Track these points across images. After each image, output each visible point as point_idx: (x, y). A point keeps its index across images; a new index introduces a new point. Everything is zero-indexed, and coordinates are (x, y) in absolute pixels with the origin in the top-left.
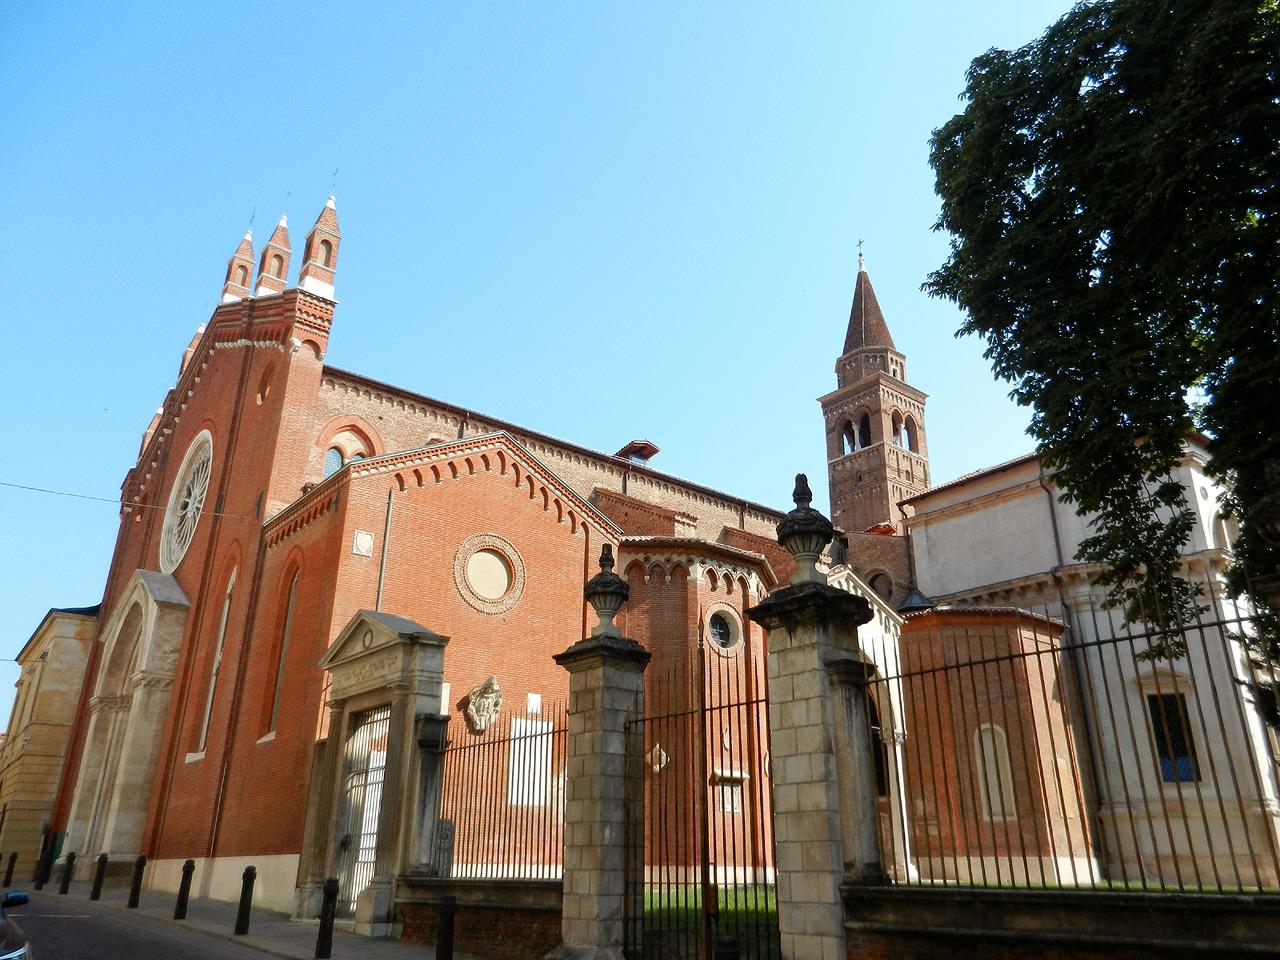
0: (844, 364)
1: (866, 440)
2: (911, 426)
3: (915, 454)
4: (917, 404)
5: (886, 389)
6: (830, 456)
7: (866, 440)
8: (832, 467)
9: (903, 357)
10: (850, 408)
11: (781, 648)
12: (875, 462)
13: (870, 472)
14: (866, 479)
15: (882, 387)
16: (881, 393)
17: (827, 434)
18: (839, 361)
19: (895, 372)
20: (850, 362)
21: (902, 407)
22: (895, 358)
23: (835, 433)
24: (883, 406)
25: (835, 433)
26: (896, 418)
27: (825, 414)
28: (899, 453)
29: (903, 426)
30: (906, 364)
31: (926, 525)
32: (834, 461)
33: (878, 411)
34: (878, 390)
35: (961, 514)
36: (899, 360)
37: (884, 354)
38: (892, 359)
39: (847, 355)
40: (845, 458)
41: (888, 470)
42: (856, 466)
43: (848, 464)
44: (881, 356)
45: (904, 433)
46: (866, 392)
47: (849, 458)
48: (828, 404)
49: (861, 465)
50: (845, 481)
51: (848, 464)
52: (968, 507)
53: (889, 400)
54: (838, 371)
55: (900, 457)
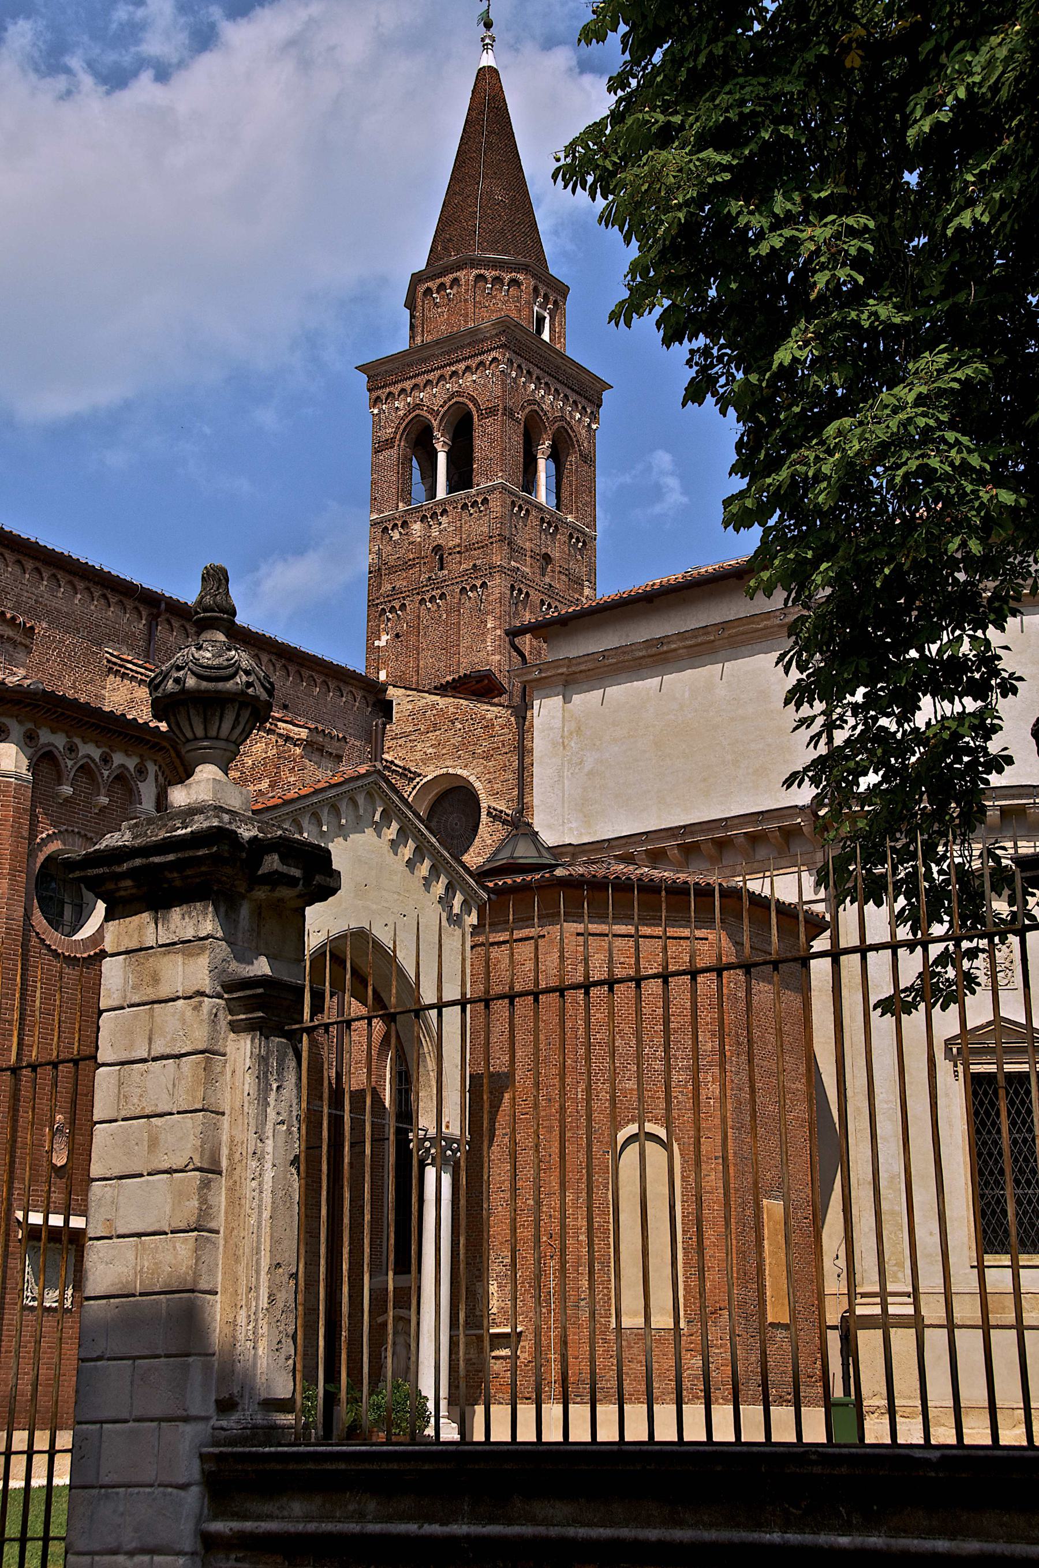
0: (429, 291)
9: (563, 291)
10: (434, 398)
11: (134, 945)
17: (377, 451)
20: (442, 287)
23: (391, 455)
25: (391, 455)
30: (570, 304)
46: (473, 363)
49: (444, 531)
50: (407, 565)
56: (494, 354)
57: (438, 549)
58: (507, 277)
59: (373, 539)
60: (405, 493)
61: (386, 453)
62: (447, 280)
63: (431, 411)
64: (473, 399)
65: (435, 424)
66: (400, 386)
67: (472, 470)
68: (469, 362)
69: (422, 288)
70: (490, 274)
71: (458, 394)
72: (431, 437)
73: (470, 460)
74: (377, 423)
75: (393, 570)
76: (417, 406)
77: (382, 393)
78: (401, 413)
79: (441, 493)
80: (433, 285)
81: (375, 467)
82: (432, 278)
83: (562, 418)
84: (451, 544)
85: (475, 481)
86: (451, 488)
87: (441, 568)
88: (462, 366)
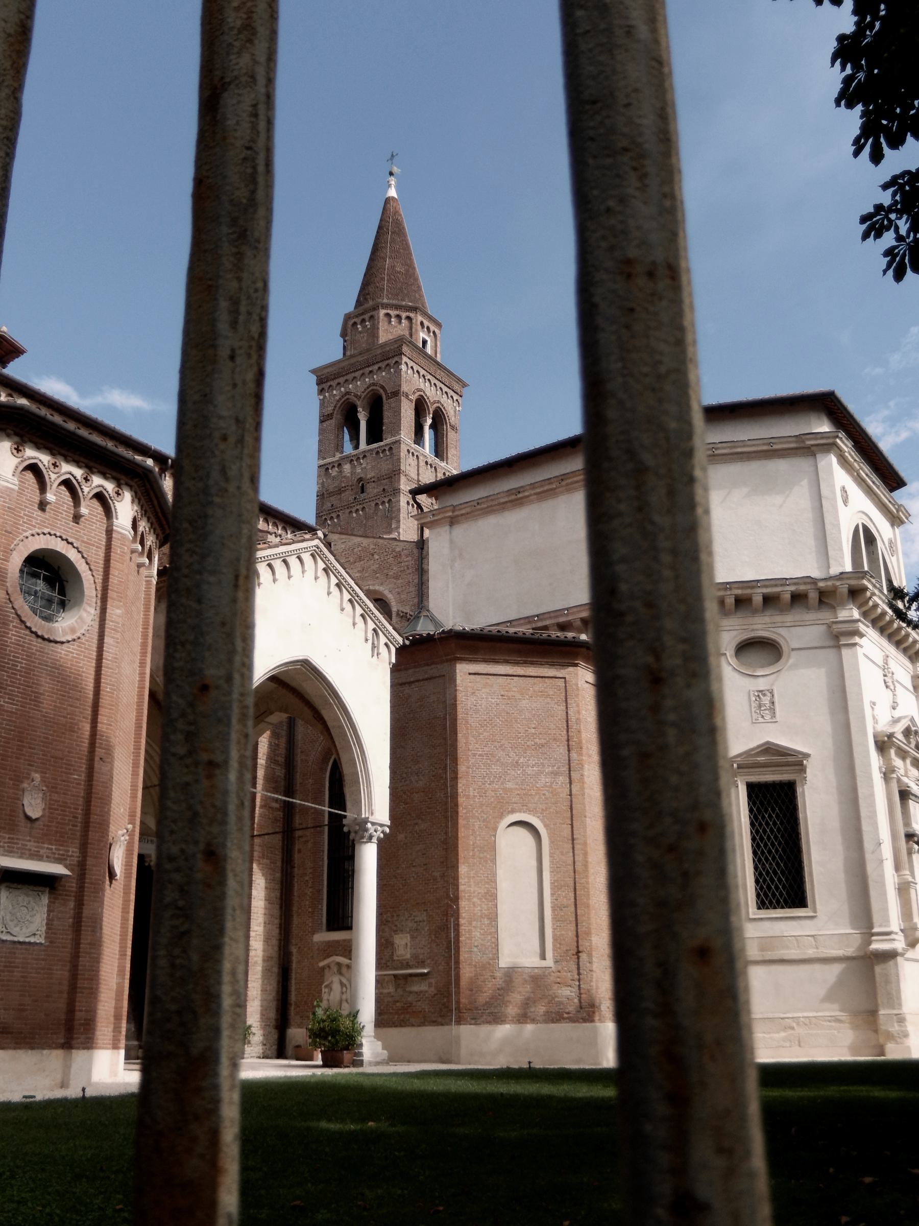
0: (355, 324)
1: (375, 435)
2: (439, 420)
3: (443, 464)
4: (451, 393)
5: (411, 363)
6: (322, 454)
7: (375, 435)
8: (324, 469)
10: (358, 387)
12: (385, 466)
13: (378, 479)
14: (372, 490)
15: (405, 359)
16: (403, 367)
17: (321, 422)
18: (348, 317)
19: (425, 342)
20: (363, 321)
21: (432, 394)
22: (426, 323)
23: (332, 423)
24: (405, 388)
25: (332, 423)
26: (420, 407)
27: (321, 391)
28: (421, 458)
29: (429, 421)
31: (452, 524)
32: (329, 460)
33: (396, 394)
34: (398, 363)
35: (504, 509)
36: (432, 328)
37: (412, 315)
38: (422, 323)
39: (361, 309)
40: (342, 459)
41: (403, 479)
42: (359, 470)
43: (347, 467)
44: (408, 318)
45: (428, 434)
46: (383, 365)
47: (350, 459)
48: (325, 378)
49: (366, 469)
50: (340, 491)
51: (347, 467)
52: (516, 500)
53: (413, 380)
54: (344, 334)
55: (422, 464)
56: (396, 359)
57: (360, 479)
58: (404, 315)
59: (319, 476)
60: (339, 447)
61: (328, 423)
62: (366, 317)
63: (356, 396)
64: (383, 387)
65: (358, 403)
66: (336, 381)
67: (382, 431)
68: (380, 365)
69: (351, 323)
70: (393, 313)
71: (374, 384)
72: (357, 411)
73: (381, 424)
74: (322, 404)
75: (331, 494)
76: (347, 393)
77: (325, 386)
78: (337, 398)
79: (363, 445)
80: (358, 320)
81: (322, 432)
82: (357, 316)
83: (439, 402)
84: (369, 476)
85: (384, 437)
86: (369, 442)
87: (363, 492)
88: (376, 367)
